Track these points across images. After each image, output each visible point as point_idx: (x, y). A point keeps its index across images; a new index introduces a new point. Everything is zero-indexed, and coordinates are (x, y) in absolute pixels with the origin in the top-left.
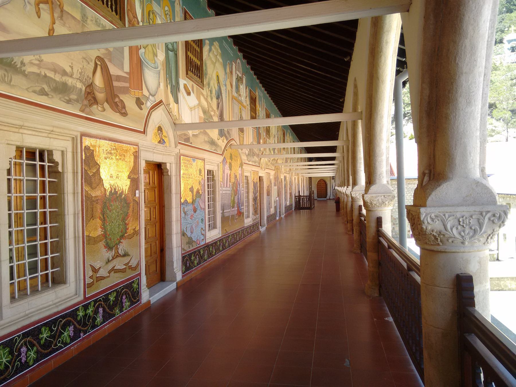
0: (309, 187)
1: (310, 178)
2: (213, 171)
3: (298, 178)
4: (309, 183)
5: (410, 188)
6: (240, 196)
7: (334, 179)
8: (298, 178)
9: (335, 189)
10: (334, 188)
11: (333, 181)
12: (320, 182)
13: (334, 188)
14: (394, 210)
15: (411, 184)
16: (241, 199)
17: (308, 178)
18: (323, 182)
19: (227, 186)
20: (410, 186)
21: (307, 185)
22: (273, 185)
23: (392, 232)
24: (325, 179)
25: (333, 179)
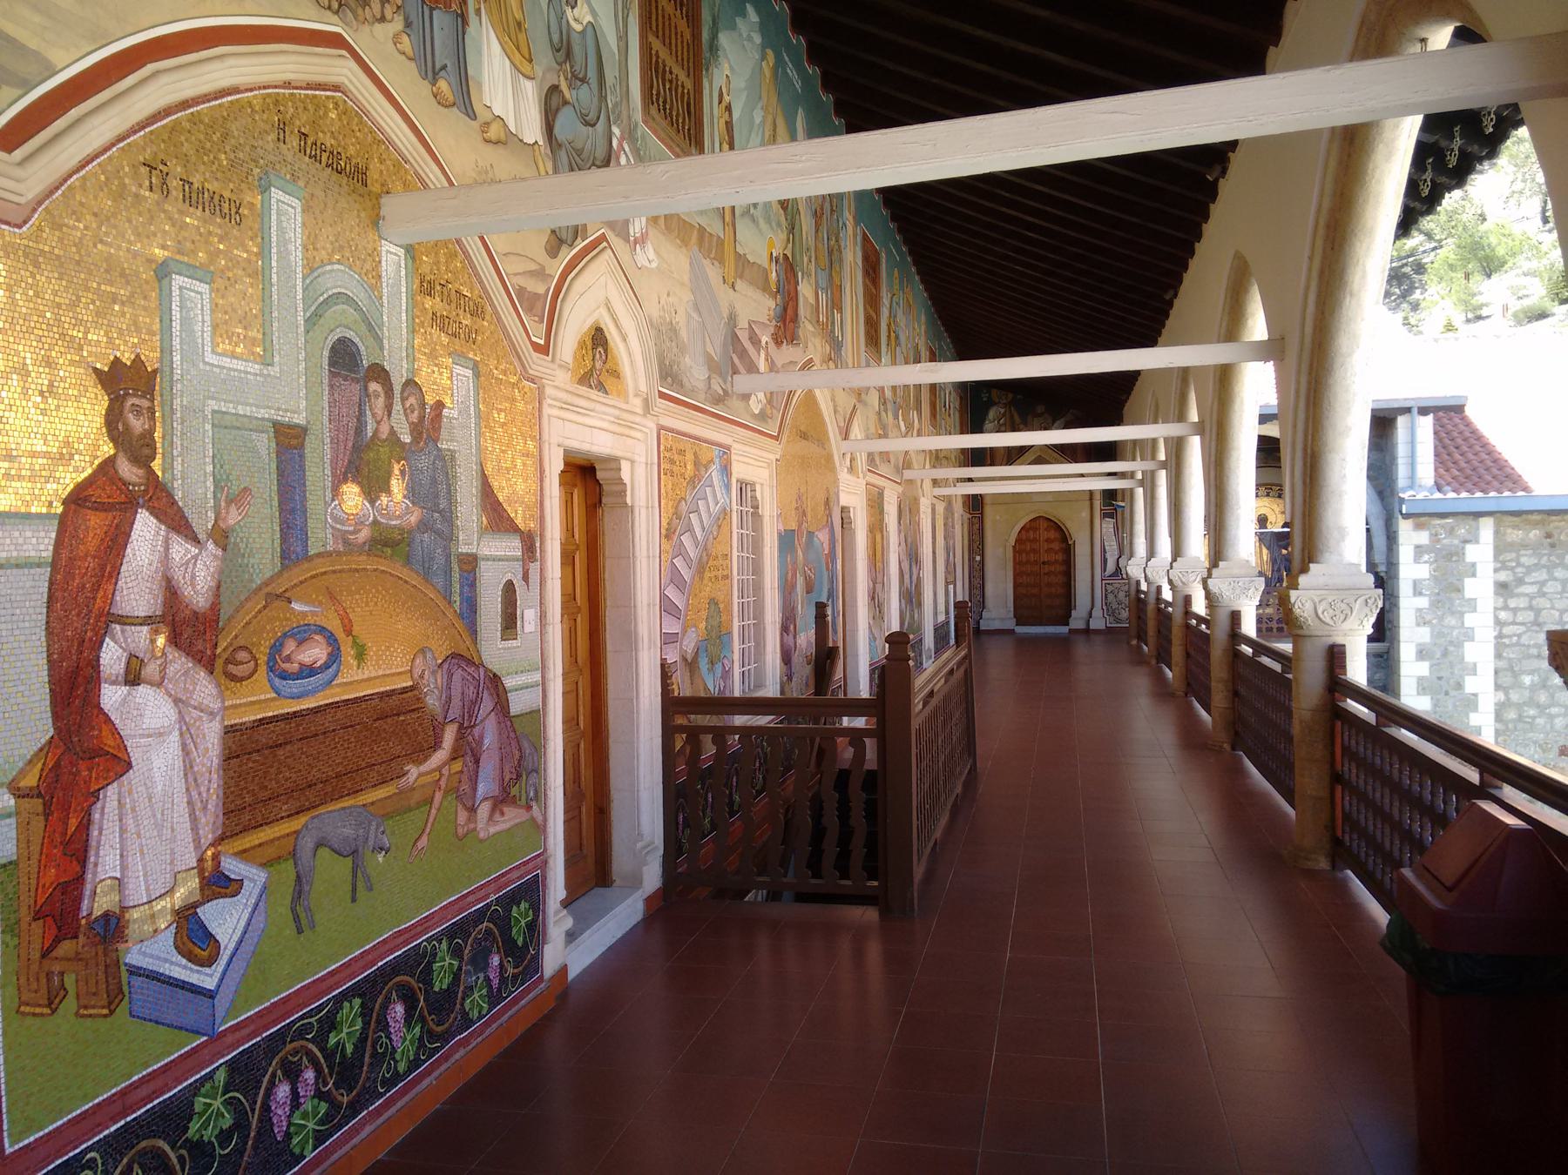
0: (971, 559)
1: (975, 504)
3: (908, 509)
4: (971, 541)
7: (1111, 516)
8: (908, 509)
9: (1118, 570)
10: (1111, 567)
11: (1109, 525)
12: (1031, 534)
13: (1111, 567)
14: (1511, 715)
17: (958, 508)
18: (1053, 534)
21: (948, 550)
24: (1061, 514)
25: (1105, 515)
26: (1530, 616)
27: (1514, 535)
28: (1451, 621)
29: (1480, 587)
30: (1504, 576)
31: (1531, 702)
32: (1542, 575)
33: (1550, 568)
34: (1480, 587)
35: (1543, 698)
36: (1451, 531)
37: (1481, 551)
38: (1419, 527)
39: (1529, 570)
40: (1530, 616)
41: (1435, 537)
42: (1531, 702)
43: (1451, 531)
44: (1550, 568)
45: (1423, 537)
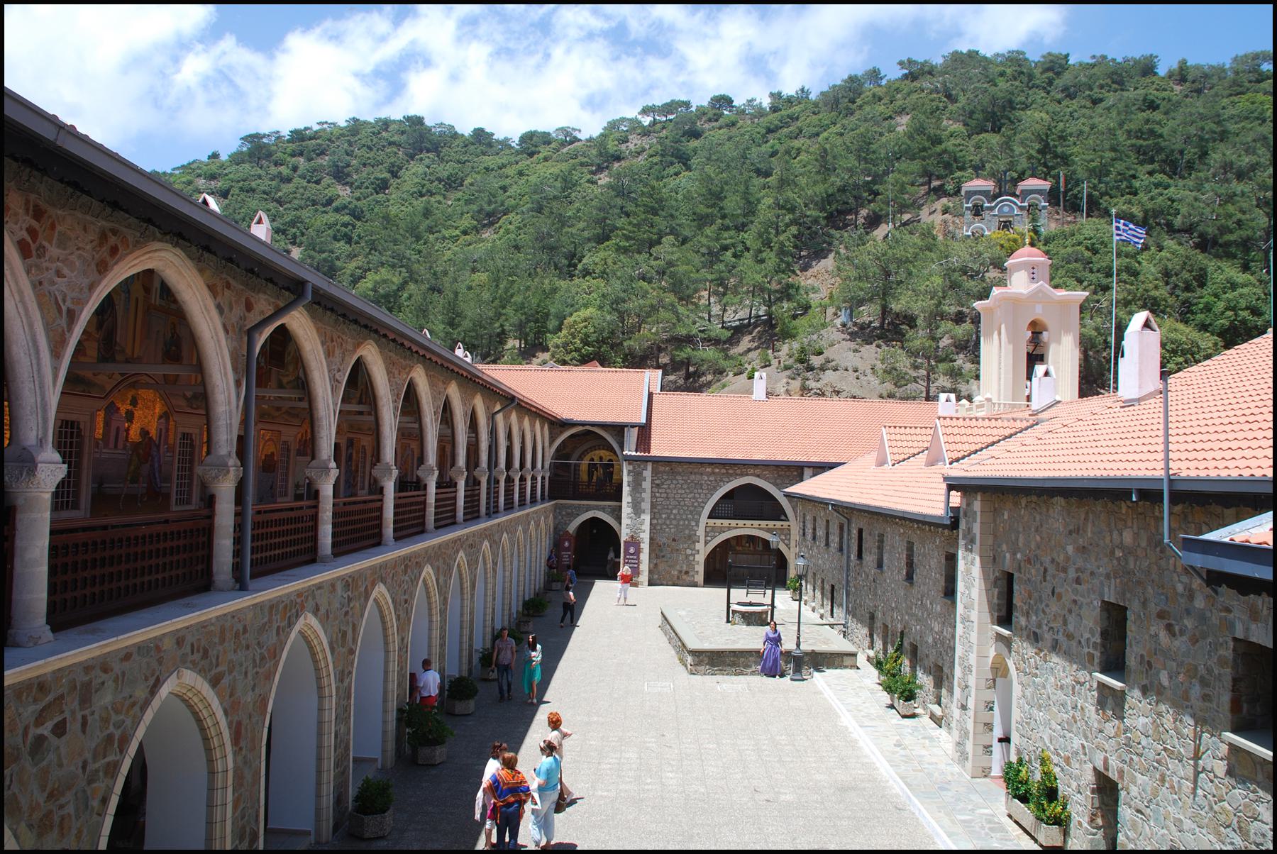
2: (78, 423)
5: (692, 482)
6: (160, 466)
15: (695, 474)
16: (160, 472)
19: (116, 447)
20: (692, 477)
22: (293, 453)
23: (650, 572)
26: (665, 495)
27: (661, 469)
28: (638, 495)
29: (647, 485)
30: (657, 482)
31: (664, 523)
32: (669, 482)
33: (672, 480)
34: (647, 485)
35: (668, 522)
36: (639, 466)
37: (648, 474)
38: (630, 464)
39: (666, 480)
40: (665, 495)
41: (634, 468)
42: (664, 523)
43: (639, 466)
44: (672, 480)
45: (631, 468)
